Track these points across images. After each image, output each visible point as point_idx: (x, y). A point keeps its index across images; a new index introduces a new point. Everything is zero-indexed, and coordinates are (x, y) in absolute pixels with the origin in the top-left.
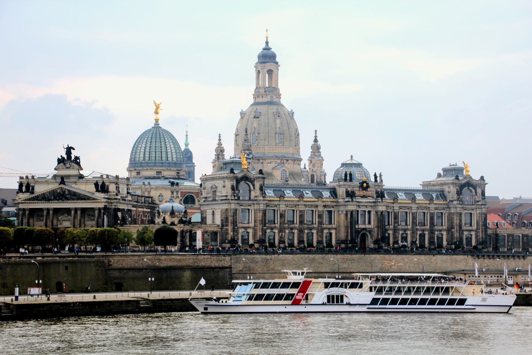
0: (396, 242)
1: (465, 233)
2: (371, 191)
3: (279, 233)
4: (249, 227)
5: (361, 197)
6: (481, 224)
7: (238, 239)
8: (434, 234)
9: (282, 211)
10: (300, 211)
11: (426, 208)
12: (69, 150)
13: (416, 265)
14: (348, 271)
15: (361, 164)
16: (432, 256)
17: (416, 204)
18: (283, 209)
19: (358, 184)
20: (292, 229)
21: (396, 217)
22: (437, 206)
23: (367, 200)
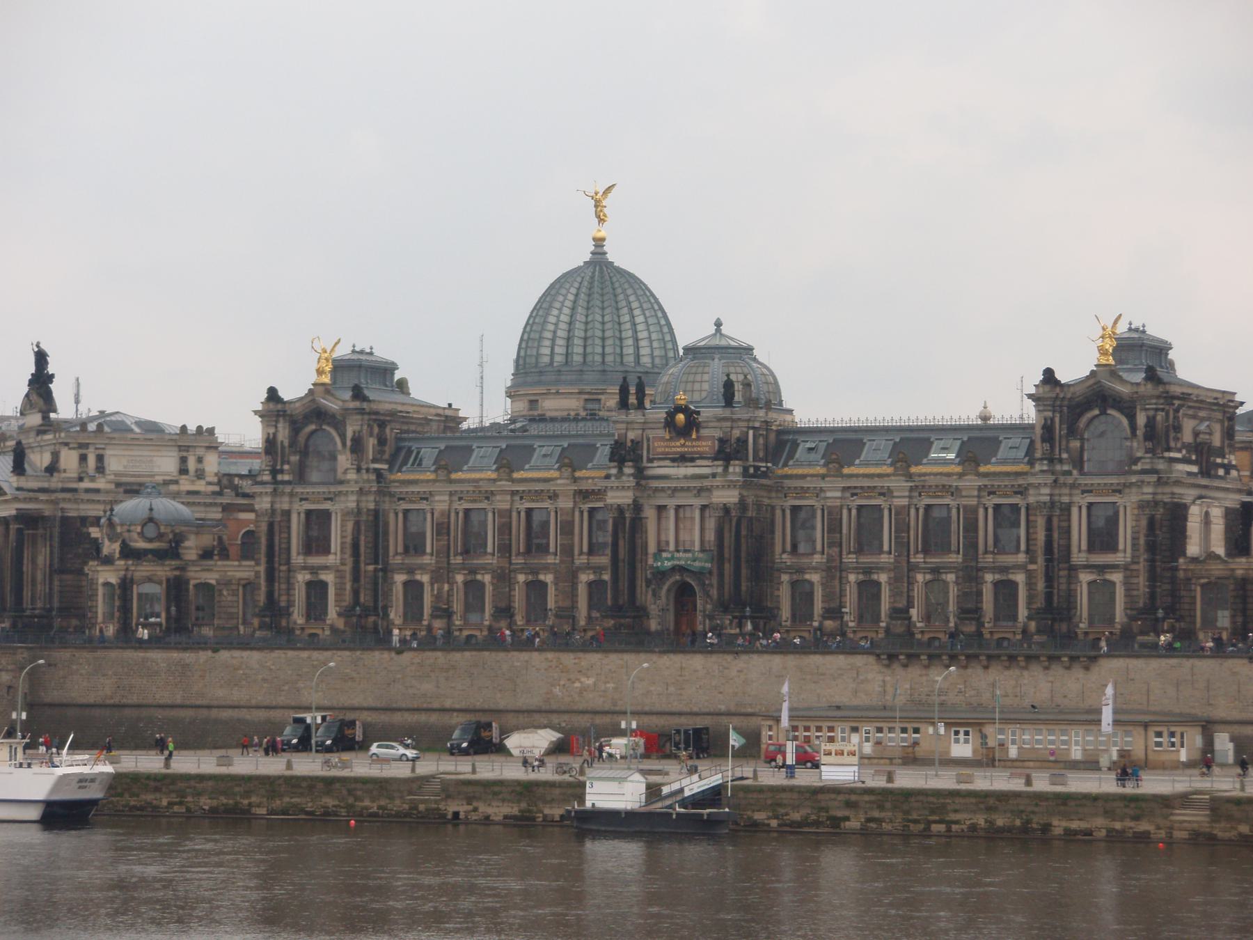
0: (834, 612)
1: (1085, 577)
2: (706, 442)
3: (432, 584)
4: (326, 568)
5: (673, 460)
6: (1142, 541)
7: (290, 604)
8: (979, 581)
9: (442, 513)
10: (502, 513)
11: (946, 490)
12: (41, 358)
13: (672, 689)
14: (436, 705)
15: (749, 350)
16: (729, 658)
17: (910, 477)
18: (445, 506)
19: (661, 415)
20: (473, 571)
21: (834, 526)
22: (985, 482)
23: (691, 471)
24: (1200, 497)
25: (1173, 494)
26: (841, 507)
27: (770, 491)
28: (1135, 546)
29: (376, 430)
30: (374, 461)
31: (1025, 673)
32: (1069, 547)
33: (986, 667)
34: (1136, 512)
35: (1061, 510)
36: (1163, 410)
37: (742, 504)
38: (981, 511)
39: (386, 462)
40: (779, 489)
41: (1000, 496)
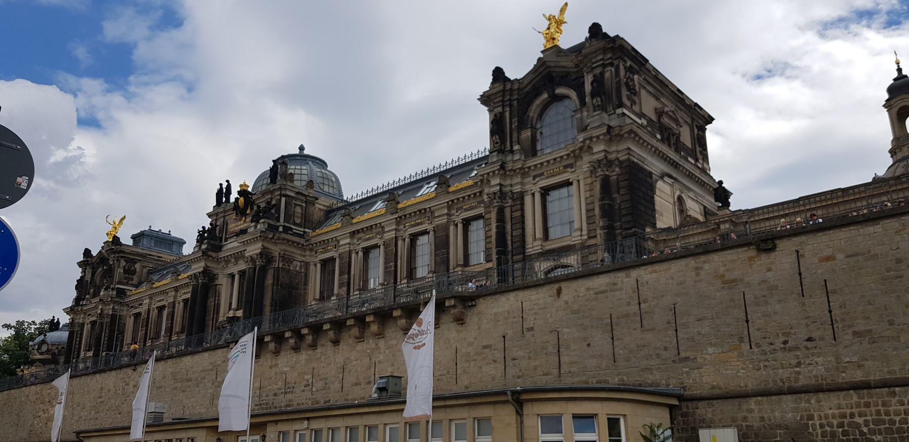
6: (597, 211)
24: (670, 177)
25: (629, 149)
26: (350, 251)
27: (305, 250)
28: (590, 218)
29: (123, 263)
30: (120, 283)
31: (382, 343)
32: (523, 235)
33: (336, 342)
34: (589, 181)
35: (513, 200)
36: (612, 64)
37: (265, 255)
38: (452, 228)
39: (134, 286)
40: (312, 248)
41: (467, 210)
